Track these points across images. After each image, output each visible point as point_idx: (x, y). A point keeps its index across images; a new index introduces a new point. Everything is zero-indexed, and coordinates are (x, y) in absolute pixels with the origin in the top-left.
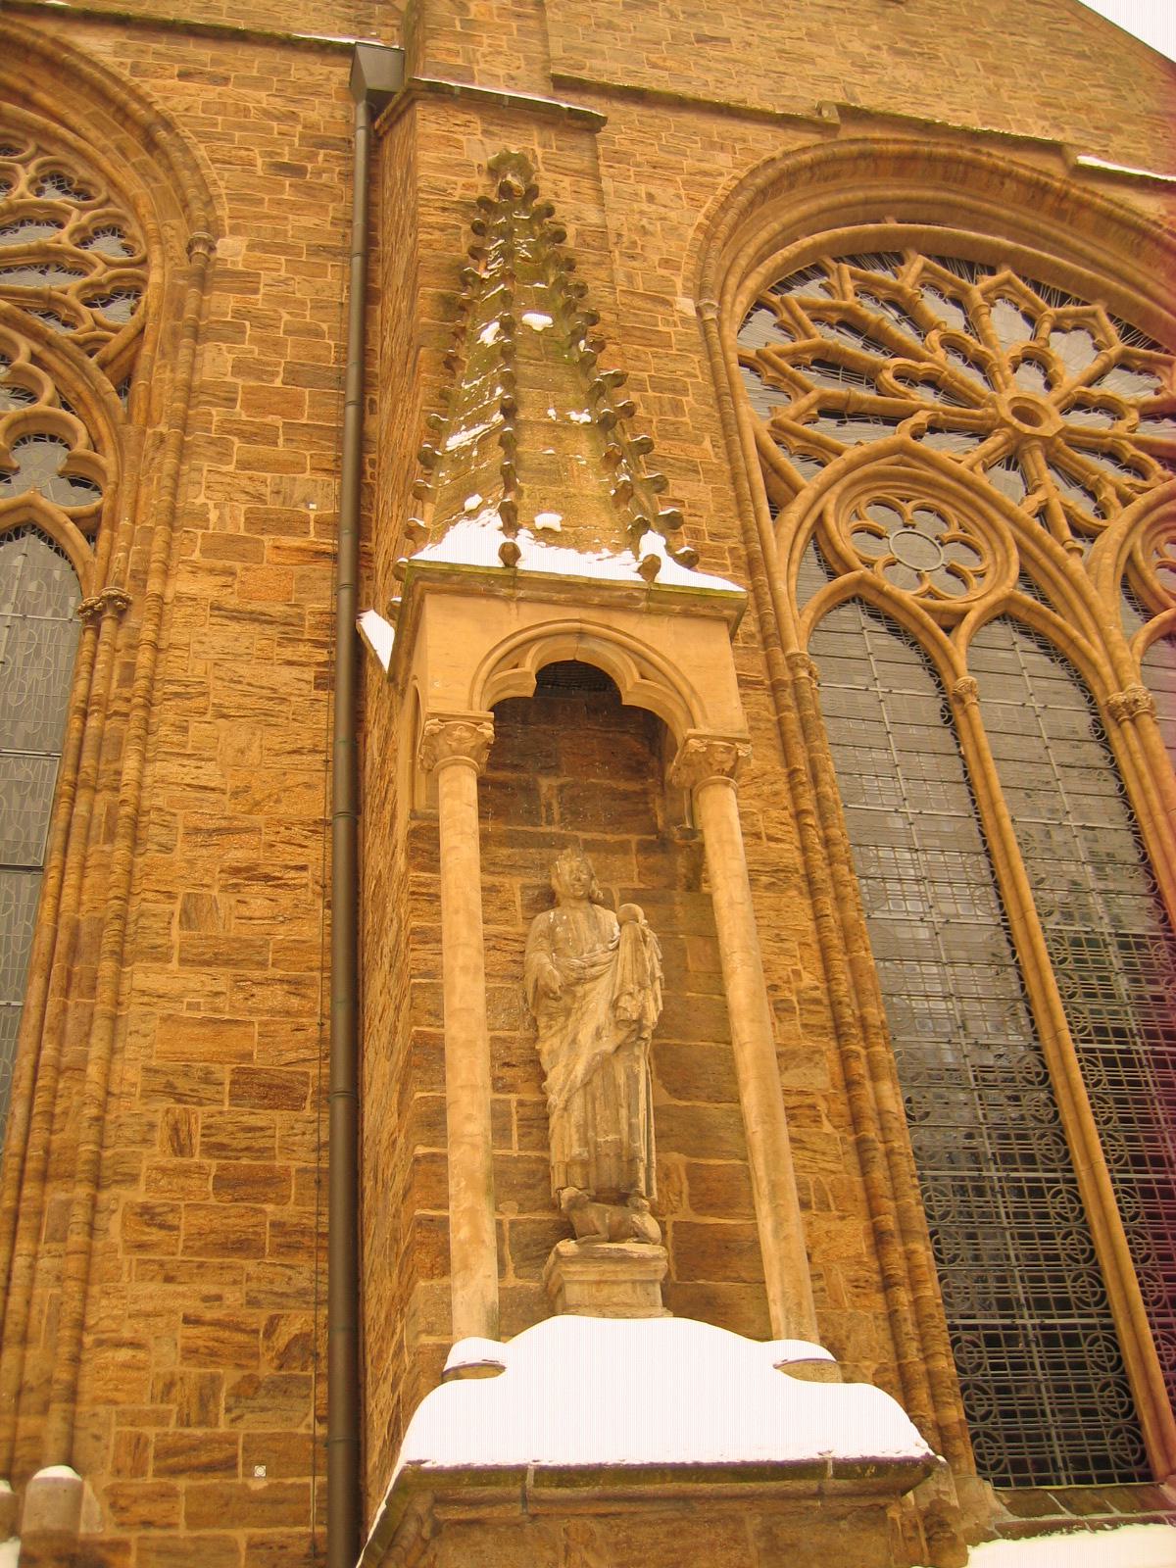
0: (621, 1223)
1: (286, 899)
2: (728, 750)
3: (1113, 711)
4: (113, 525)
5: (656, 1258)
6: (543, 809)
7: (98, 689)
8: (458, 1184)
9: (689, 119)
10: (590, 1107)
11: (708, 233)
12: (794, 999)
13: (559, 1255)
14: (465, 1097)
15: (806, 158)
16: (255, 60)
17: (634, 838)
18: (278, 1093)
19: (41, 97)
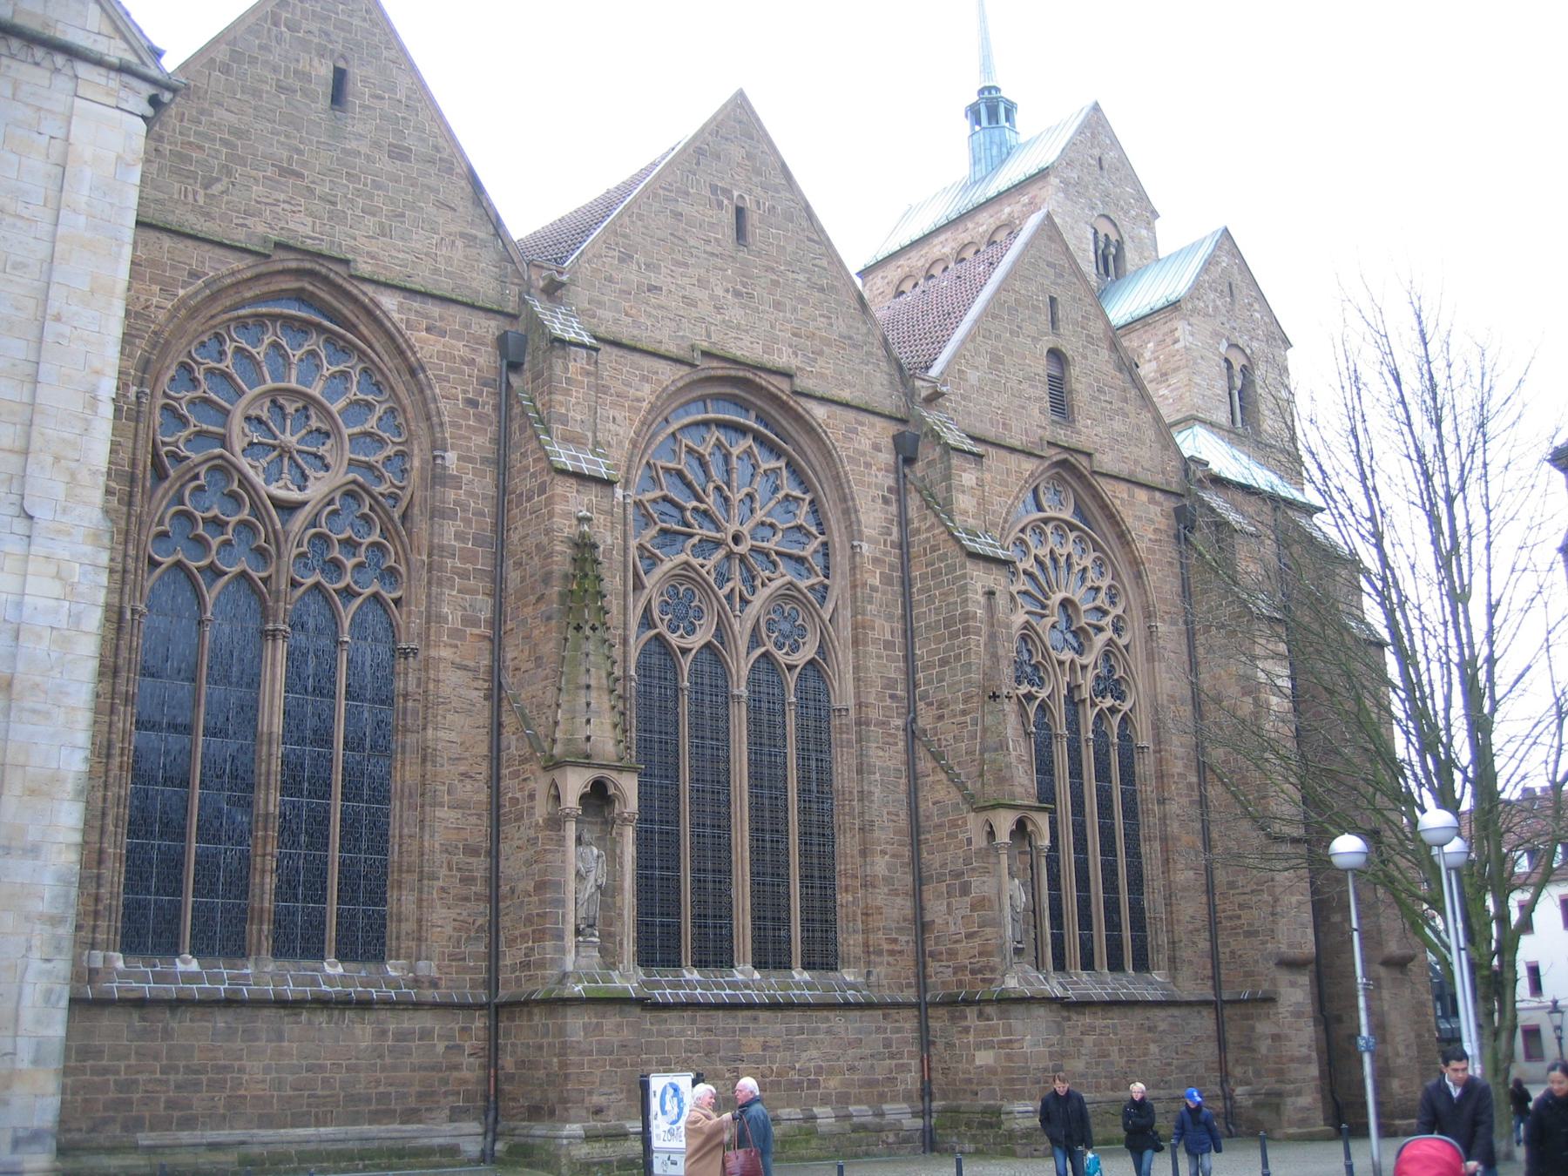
1: (476, 785)
3: (733, 696)
4: (409, 604)
7: (410, 689)
9: (636, 357)
11: (634, 444)
15: (680, 384)
16: (458, 315)
17: (599, 820)
18: (472, 851)
19: (362, 328)
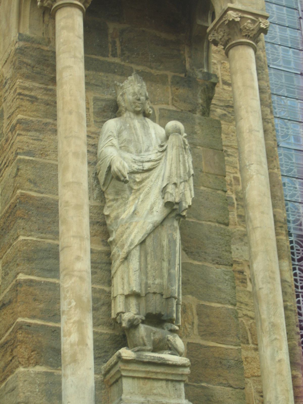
0: (161, 341)
2: (254, 22)
5: (183, 366)
6: (110, 45)
8: (70, 303)
10: (143, 258)
12: (234, 196)
13: (119, 357)
14: (75, 244)
17: (170, 74)
